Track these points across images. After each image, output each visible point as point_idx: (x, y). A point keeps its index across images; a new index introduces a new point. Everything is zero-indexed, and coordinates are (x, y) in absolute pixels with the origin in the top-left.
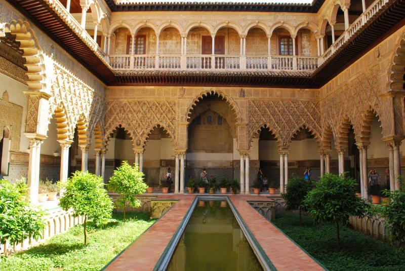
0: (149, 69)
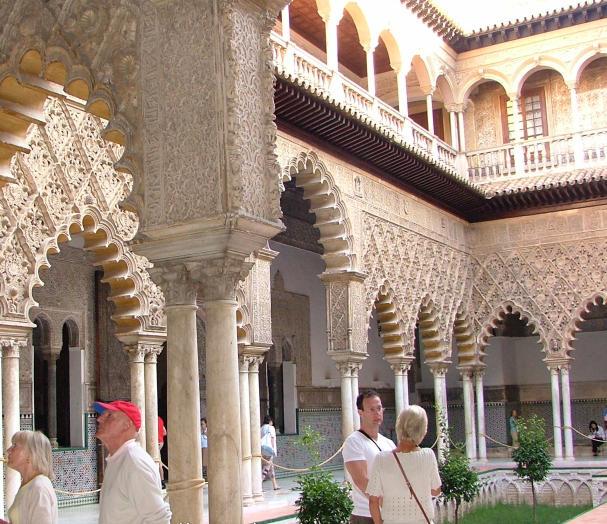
0: (561, 170)
